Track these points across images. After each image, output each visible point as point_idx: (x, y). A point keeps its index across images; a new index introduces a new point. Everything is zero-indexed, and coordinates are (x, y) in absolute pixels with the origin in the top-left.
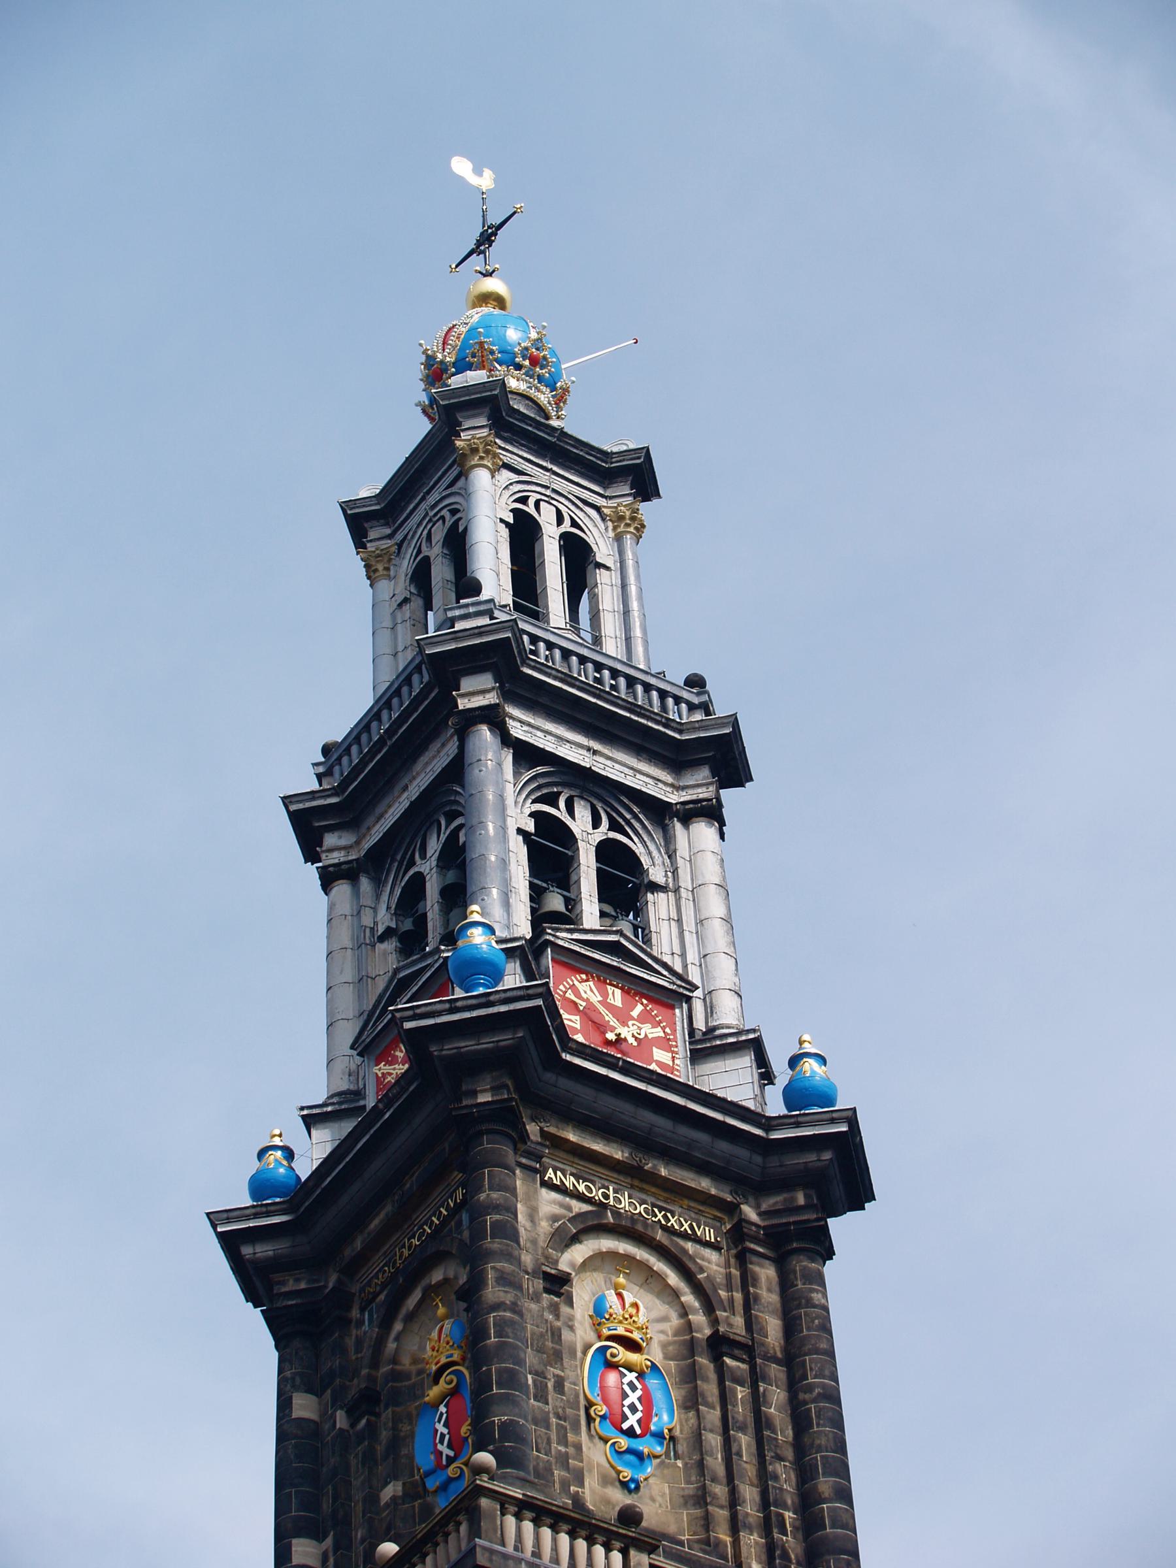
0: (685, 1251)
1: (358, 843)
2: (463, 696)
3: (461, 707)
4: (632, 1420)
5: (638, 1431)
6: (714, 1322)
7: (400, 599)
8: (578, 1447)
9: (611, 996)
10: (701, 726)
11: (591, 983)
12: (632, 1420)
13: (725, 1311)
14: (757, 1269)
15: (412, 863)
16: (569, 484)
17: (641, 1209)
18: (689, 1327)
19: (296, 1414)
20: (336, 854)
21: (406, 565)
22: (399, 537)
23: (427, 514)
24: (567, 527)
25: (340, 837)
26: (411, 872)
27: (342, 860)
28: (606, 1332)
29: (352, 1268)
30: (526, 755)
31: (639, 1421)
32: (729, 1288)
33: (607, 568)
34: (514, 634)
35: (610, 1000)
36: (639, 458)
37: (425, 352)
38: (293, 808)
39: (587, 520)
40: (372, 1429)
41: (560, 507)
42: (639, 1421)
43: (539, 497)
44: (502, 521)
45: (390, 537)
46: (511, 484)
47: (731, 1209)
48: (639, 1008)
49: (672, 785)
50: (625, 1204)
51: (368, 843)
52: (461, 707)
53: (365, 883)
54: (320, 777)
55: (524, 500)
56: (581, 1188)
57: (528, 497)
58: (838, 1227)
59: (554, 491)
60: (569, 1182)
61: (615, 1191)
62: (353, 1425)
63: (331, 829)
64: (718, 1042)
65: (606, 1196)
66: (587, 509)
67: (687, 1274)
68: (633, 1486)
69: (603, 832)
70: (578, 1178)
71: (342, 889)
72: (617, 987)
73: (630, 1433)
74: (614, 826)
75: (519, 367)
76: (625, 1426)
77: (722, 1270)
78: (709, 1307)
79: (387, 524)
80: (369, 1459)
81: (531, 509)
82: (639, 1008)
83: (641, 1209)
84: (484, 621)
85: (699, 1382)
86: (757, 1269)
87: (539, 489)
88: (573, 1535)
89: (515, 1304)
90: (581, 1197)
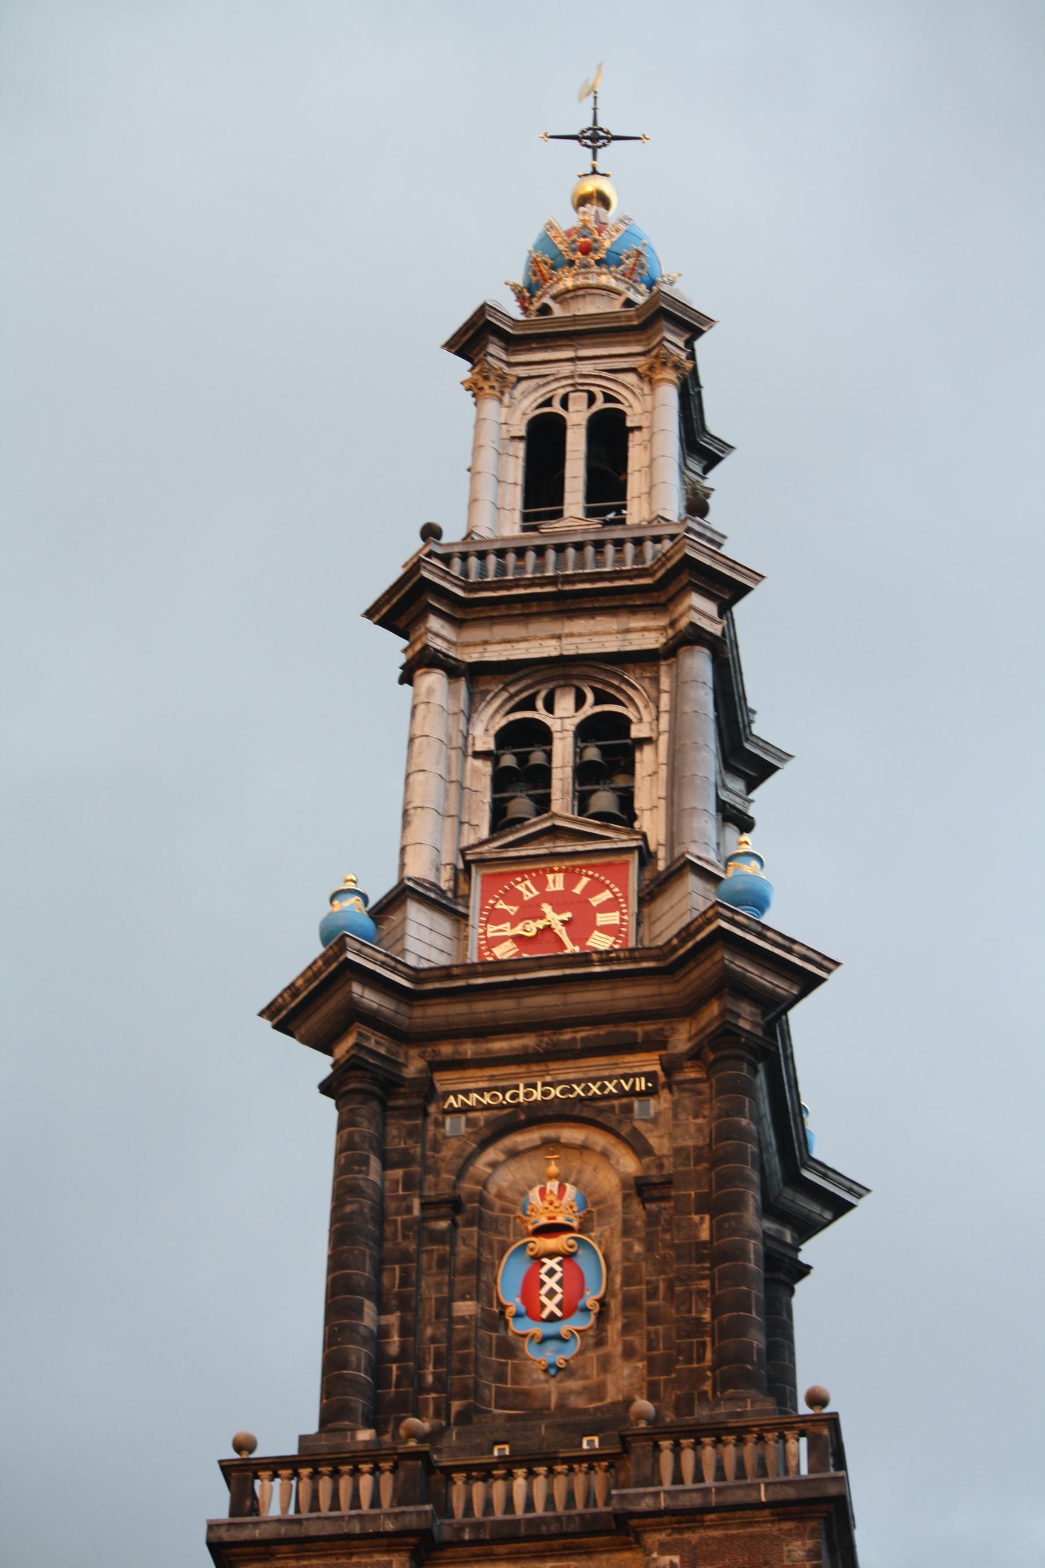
4: (551, 1306)
5: (559, 1313)
9: (551, 884)
11: (528, 883)
12: (551, 1306)
17: (555, 1092)
28: (531, 1228)
30: (477, 676)
31: (559, 1305)
35: (551, 888)
42: (559, 1305)
48: (585, 880)
50: (537, 1095)
56: (487, 1100)
60: (472, 1100)
61: (526, 1086)
65: (514, 1096)
68: (552, 1371)
69: (589, 709)
70: (481, 1092)
72: (559, 871)
73: (552, 1318)
74: (601, 698)
76: (544, 1315)
82: (585, 880)
83: (555, 1092)
90: (488, 1107)
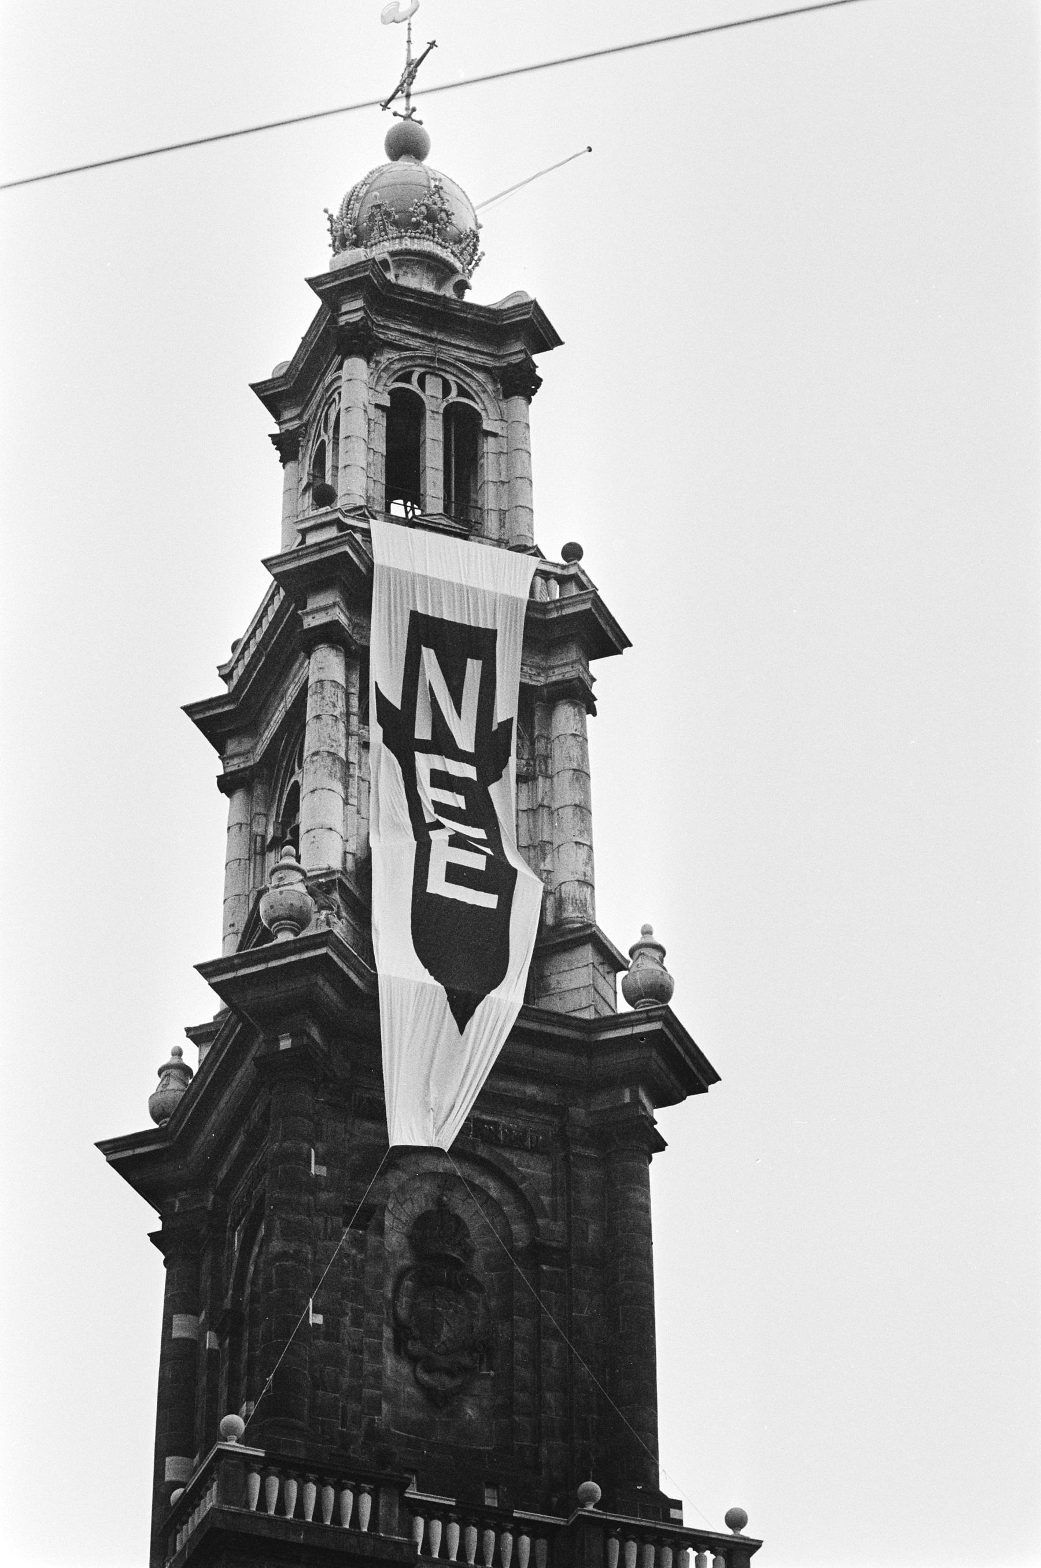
0: (509, 1163)
1: (254, 748)
2: (307, 614)
3: (306, 627)
6: (535, 1229)
7: (304, 482)
8: (378, 1375)
10: (573, 600)
13: (546, 1216)
14: (582, 1173)
15: (293, 773)
16: (459, 350)
18: (509, 1237)
19: (175, 1334)
20: (236, 761)
21: (309, 451)
22: (306, 417)
23: (323, 396)
24: (453, 396)
25: (240, 743)
26: (292, 781)
27: (242, 766)
29: (224, 1191)
32: (553, 1192)
33: (495, 435)
34: (352, 547)
36: (527, 313)
37: (330, 218)
38: (197, 717)
39: (474, 385)
40: (235, 1350)
41: (448, 377)
43: (422, 370)
44: (377, 406)
45: (299, 416)
46: (391, 363)
47: (560, 1112)
49: (538, 667)
51: (261, 749)
52: (306, 627)
53: (259, 791)
54: (226, 678)
55: (406, 378)
57: (412, 372)
58: (666, 1119)
59: (440, 361)
62: (221, 1345)
63: (233, 734)
64: (570, 937)
66: (476, 374)
67: (509, 1184)
71: (239, 796)
75: (417, 225)
77: (550, 1176)
78: (530, 1214)
79: (297, 405)
80: (233, 1378)
81: (414, 387)
84: (332, 532)
85: (516, 1293)
86: (582, 1173)
87: (424, 362)
88: (321, 1484)
89: (298, 1252)
